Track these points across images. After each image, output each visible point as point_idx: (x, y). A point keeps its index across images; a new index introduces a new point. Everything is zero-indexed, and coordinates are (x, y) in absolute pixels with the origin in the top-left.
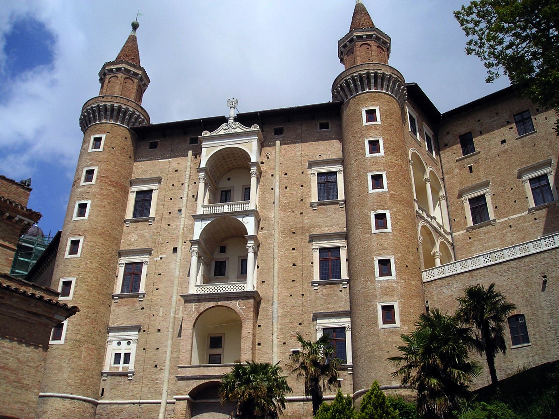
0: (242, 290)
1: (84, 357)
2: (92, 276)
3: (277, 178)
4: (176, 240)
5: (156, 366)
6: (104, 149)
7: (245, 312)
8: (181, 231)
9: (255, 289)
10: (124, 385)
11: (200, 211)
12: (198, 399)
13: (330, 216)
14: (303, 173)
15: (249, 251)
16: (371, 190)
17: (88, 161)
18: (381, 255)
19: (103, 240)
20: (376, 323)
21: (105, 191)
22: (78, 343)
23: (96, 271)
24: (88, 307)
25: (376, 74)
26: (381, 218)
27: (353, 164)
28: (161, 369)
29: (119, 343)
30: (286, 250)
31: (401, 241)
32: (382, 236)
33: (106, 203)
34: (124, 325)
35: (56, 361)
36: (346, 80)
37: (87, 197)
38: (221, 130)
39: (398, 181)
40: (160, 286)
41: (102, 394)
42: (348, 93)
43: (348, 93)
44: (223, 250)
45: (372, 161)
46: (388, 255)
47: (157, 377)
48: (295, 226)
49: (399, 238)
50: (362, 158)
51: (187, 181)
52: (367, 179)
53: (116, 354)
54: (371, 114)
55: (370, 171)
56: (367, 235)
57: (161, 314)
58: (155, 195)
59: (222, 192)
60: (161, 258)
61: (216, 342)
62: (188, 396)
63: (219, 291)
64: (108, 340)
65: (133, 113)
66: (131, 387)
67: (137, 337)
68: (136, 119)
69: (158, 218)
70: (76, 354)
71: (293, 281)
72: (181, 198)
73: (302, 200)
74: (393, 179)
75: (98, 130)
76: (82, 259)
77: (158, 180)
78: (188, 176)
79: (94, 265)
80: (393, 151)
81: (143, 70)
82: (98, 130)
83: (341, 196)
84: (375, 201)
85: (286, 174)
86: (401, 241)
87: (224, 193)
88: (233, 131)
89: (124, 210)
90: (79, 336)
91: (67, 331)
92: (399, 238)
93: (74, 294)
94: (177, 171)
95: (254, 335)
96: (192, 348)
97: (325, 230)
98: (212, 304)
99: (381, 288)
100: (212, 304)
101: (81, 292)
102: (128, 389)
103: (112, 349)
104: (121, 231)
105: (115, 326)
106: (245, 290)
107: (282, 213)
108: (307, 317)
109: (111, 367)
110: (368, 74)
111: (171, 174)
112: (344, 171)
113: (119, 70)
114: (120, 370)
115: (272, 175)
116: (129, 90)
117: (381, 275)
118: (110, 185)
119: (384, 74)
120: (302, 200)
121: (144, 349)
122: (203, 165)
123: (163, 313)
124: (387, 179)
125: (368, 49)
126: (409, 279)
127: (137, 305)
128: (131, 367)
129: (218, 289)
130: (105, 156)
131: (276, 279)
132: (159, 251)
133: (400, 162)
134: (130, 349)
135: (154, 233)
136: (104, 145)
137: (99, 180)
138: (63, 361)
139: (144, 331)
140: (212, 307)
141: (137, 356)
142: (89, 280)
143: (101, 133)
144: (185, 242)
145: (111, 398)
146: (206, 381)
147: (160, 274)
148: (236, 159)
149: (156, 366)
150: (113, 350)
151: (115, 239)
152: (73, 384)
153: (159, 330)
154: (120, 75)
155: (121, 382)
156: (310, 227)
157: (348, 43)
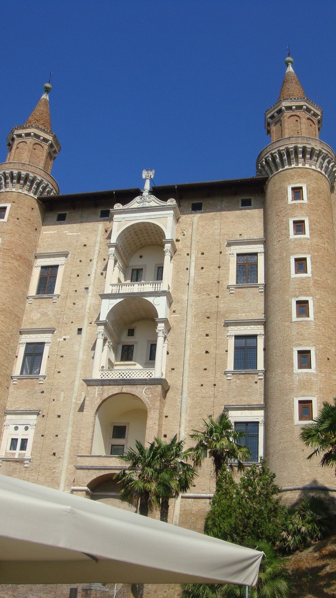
0: (149, 377)
3: (193, 258)
6: (8, 220)
7: (151, 401)
8: (87, 310)
9: (164, 377)
10: (20, 472)
11: (108, 290)
12: (96, 492)
14: (221, 253)
15: (159, 335)
16: (293, 275)
18: (301, 345)
19: (3, 317)
20: (292, 419)
21: (7, 265)
25: (304, 148)
26: (303, 306)
27: (276, 245)
28: (59, 458)
29: (16, 428)
30: (199, 336)
31: (324, 331)
32: (303, 325)
33: (8, 278)
34: (22, 409)
36: (272, 154)
38: (135, 203)
39: (323, 266)
40: (61, 369)
42: (273, 168)
43: (273, 168)
44: (131, 333)
45: (296, 242)
46: (309, 345)
47: (55, 466)
48: (210, 311)
49: (321, 328)
50: (285, 239)
52: (290, 262)
53: (13, 439)
54: (297, 192)
55: (293, 254)
56: (287, 324)
57: (62, 399)
58: (60, 271)
59: (133, 270)
60: (65, 339)
61: (119, 432)
62: (86, 488)
63: (125, 377)
64: (5, 424)
65: (41, 182)
66: (27, 475)
68: (44, 189)
69: (63, 295)
71: (205, 369)
72: (89, 275)
73: (218, 282)
74: (318, 264)
75: (3, 199)
77: (66, 255)
78: (97, 252)
80: (319, 233)
82: (3, 199)
83: (261, 279)
84: (297, 286)
85: (203, 254)
86: (324, 331)
87: (135, 272)
88: (147, 205)
89: (27, 286)
92: (321, 328)
94: (85, 245)
95: (160, 426)
96: (93, 437)
97: (243, 316)
98: (116, 390)
99: (299, 381)
100: (116, 390)
102: (24, 477)
103: (9, 433)
104: (23, 308)
105: (13, 409)
106: (153, 377)
107: (197, 296)
108: (218, 409)
109: (6, 453)
110: (296, 148)
112: (266, 253)
113: (28, 135)
114: (16, 457)
115: (188, 254)
116: (39, 157)
117: (300, 367)
118: (13, 258)
119: (313, 149)
120: (218, 282)
121: (43, 436)
122: (114, 240)
123: (64, 397)
124: (312, 263)
125: (297, 121)
126: (329, 373)
127: (36, 388)
128: (28, 453)
129: (123, 375)
130: (10, 228)
131: (186, 366)
132: (63, 331)
133: (326, 245)
134: (28, 435)
136: (9, 215)
139: (43, 416)
140: (117, 394)
141: (34, 442)
143: (6, 202)
144: (91, 323)
146: (107, 472)
147: (62, 356)
148: (149, 236)
149: (54, 454)
150: (9, 435)
151: (16, 316)
153: (59, 416)
154: (30, 140)
155: (16, 469)
156: (226, 312)
157: (276, 114)
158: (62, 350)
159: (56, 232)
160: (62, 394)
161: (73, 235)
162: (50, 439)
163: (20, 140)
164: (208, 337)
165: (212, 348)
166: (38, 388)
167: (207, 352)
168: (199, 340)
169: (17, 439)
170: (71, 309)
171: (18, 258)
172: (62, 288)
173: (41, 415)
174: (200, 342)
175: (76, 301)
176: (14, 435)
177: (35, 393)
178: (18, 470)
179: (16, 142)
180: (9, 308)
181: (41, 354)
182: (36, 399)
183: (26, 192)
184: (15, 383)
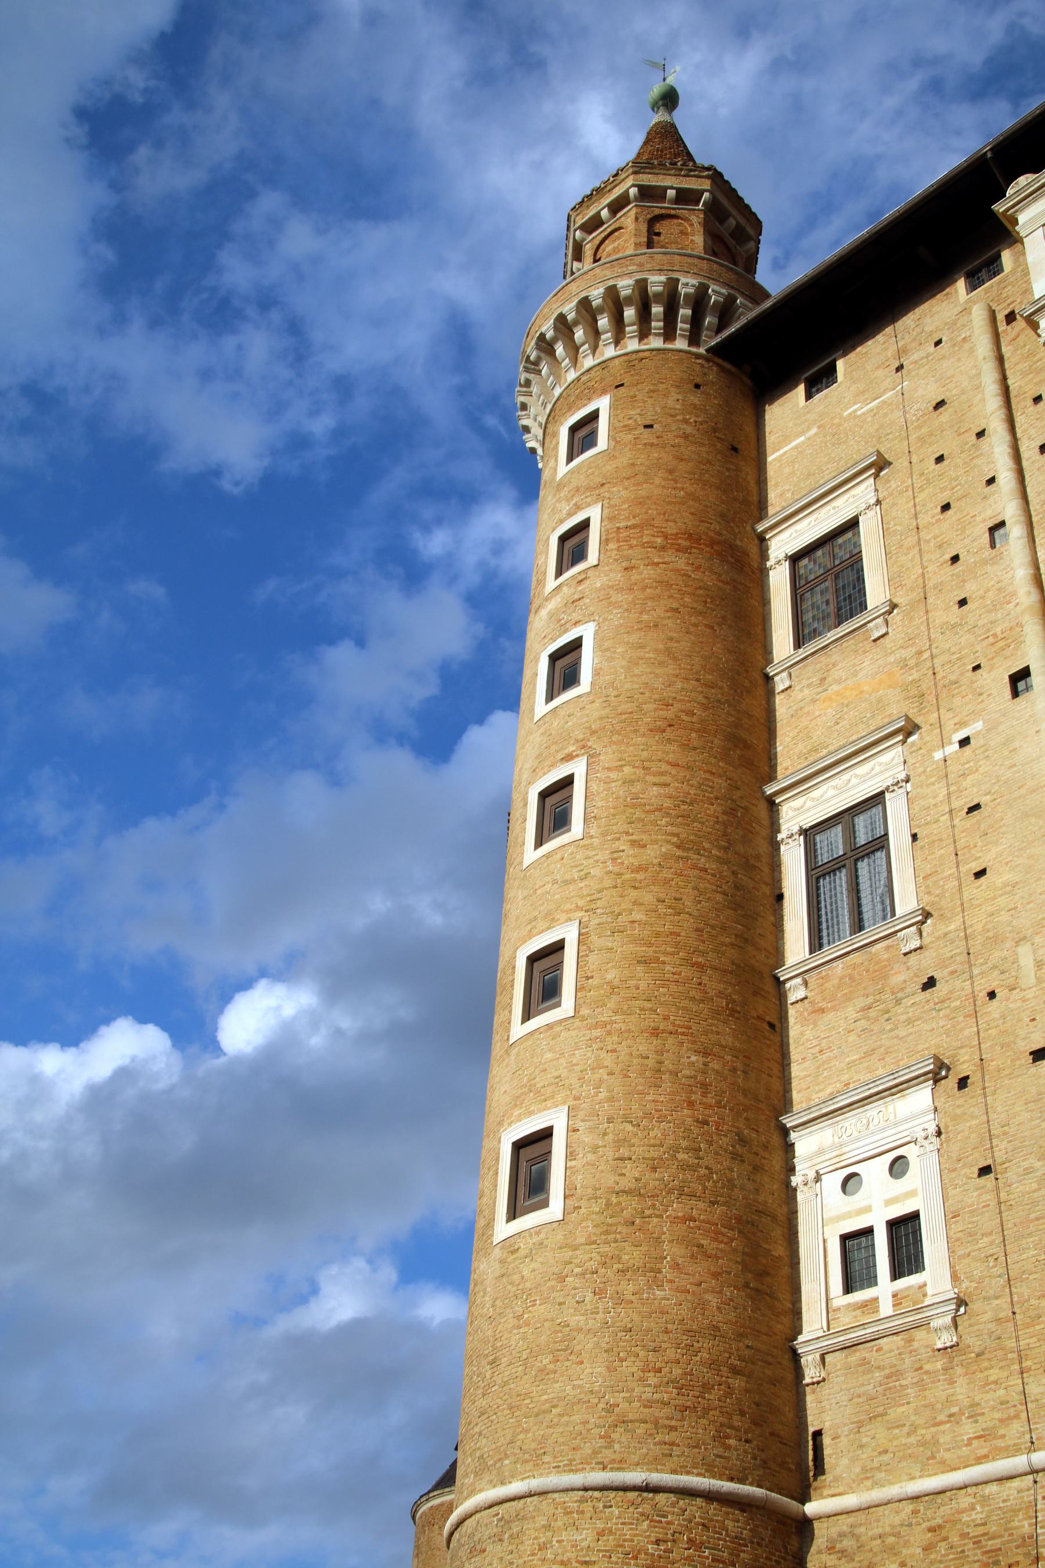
1: (676, 1266)
2: (648, 898)
4: (1012, 639)
10: (921, 1385)
17: (564, 504)
19: (674, 747)
22: (632, 1204)
23: (666, 874)
24: (655, 1032)
33: (660, 612)
35: (540, 1310)
37: (575, 616)
41: (820, 1468)
51: (993, 403)
58: (870, 540)
60: (964, 742)
66: (962, 1390)
70: (632, 1256)
76: (596, 841)
79: (652, 853)
81: (717, 177)
90: (632, 1171)
91: (570, 1155)
101: (609, 977)
111: (919, 427)
118: (663, 548)
121: (985, 1171)
127: (897, 979)
128: (935, 1277)
130: (623, 460)
132: (946, 716)
134: (912, 1194)
135: (904, 664)
137: (612, 546)
138: (570, 1301)
139: (963, 1083)
141: (951, 1216)
142: (638, 916)
145: (867, 1476)
147: (974, 808)
152: (635, 1411)
155: (898, 1374)
159: (814, 430)
160: (1026, 957)
161: (884, 402)
162: (1028, 1171)
163: (598, 234)
166: (905, 976)
170: (954, 626)
171: (684, 543)
172: (894, 581)
173: (952, 1082)
175: (969, 590)
177: (898, 1002)
178: (909, 1378)
179: (588, 250)
180: (691, 713)
181: (880, 843)
182: (909, 1022)
183: (656, 342)
184: (801, 993)
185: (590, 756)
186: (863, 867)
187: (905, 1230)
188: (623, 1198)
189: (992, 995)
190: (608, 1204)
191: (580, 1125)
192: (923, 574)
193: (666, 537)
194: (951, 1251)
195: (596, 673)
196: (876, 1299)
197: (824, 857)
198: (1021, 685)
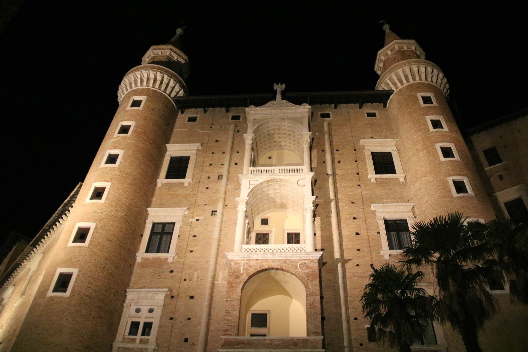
4: (215, 202)
5: (186, 340)
13: (391, 189)
28: (194, 344)
29: (138, 311)
44: (265, 222)
51: (229, 148)
55: (438, 142)
60: (197, 220)
64: (125, 305)
67: (162, 303)
70: (84, 312)
71: (358, 250)
79: (120, 214)
93: (91, 241)
101: (100, 240)
103: (129, 315)
121: (171, 319)
123: (198, 277)
134: (152, 318)
139: (172, 297)
141: (160, 326)
150: (129, 317)
158: (196, 229)
159: (187, 129)
160: (196, 273)
162: (181, 322)
164: (355, 220)
165: (362, 229)
167: (357, 234)
168: (347, 223)
169: (138, 324)
174: (349, 224)
175: (210, 186)
176: (135, 317)
177: (163, 272)
181: (171, 234)
185: (112, 183)
186: (164, 237)
187: (148, 326)
188: (86, 298)
189: (185, 280)
190: (82, 298)
191: (81, 275)
192: (200, 177)
193: (148, 138)
194: (158, 334)
195: (121, 163)
196: (135, 339)
197: (155, 231)
198: (214, 213)
